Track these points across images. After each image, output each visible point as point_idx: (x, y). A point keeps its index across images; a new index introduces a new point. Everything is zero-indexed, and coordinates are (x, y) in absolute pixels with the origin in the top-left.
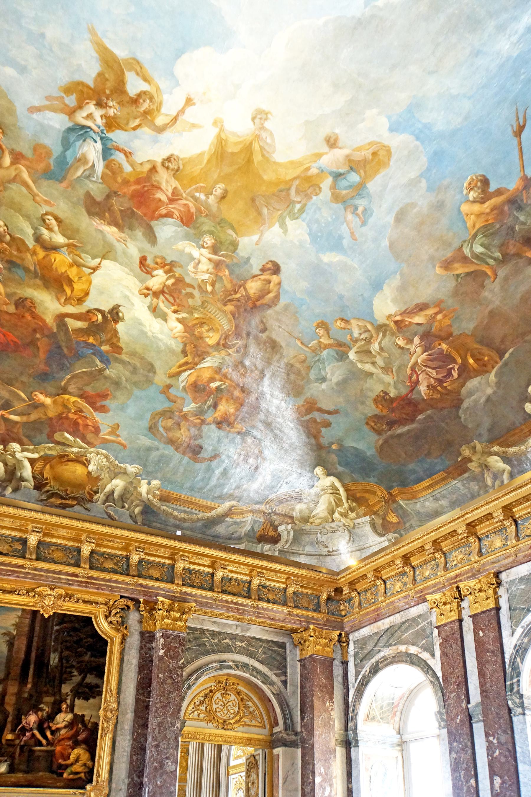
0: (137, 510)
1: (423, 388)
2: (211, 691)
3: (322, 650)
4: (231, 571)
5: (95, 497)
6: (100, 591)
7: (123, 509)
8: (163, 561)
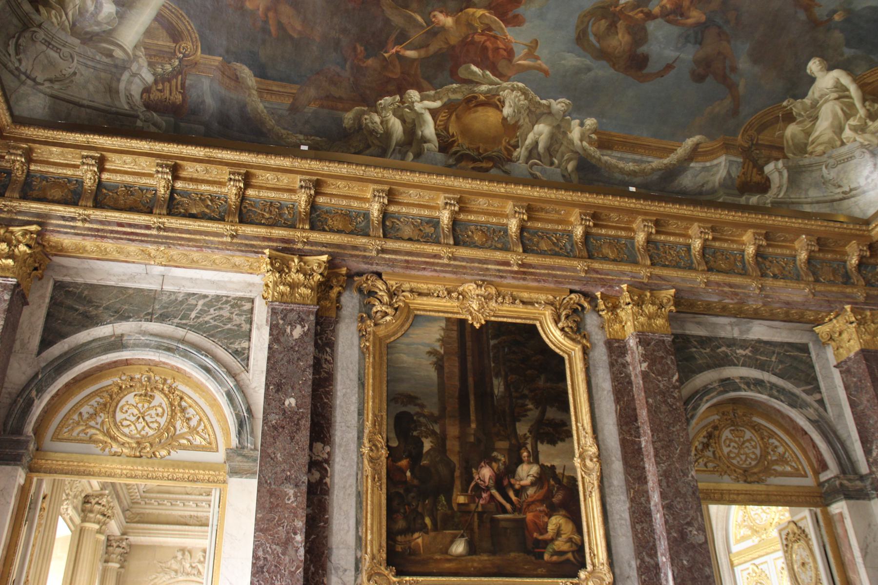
0: (570, 167)
2: (715, 428)
5: (515, 154)
6: (542, 284)
7: (553, 168)
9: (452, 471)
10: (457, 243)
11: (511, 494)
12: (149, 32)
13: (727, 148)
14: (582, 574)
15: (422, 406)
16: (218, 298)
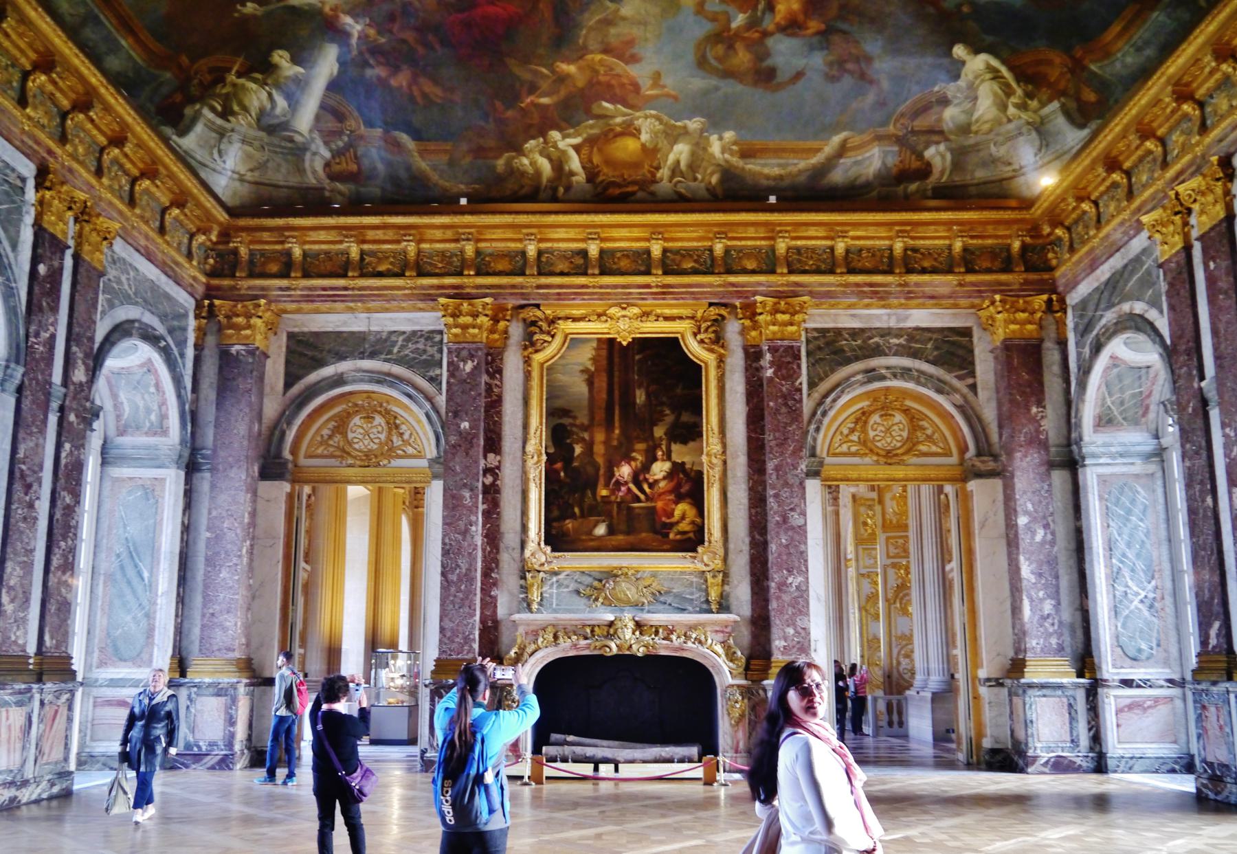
3: (1021, 330)
4: (853, 238)
8: (758, 243)
9: (598, 470)
11: (646, 487)
12: (318, 118)
13: (879, 138)
14: (700, 549)
15: (575, 418)
16: (414, 333)
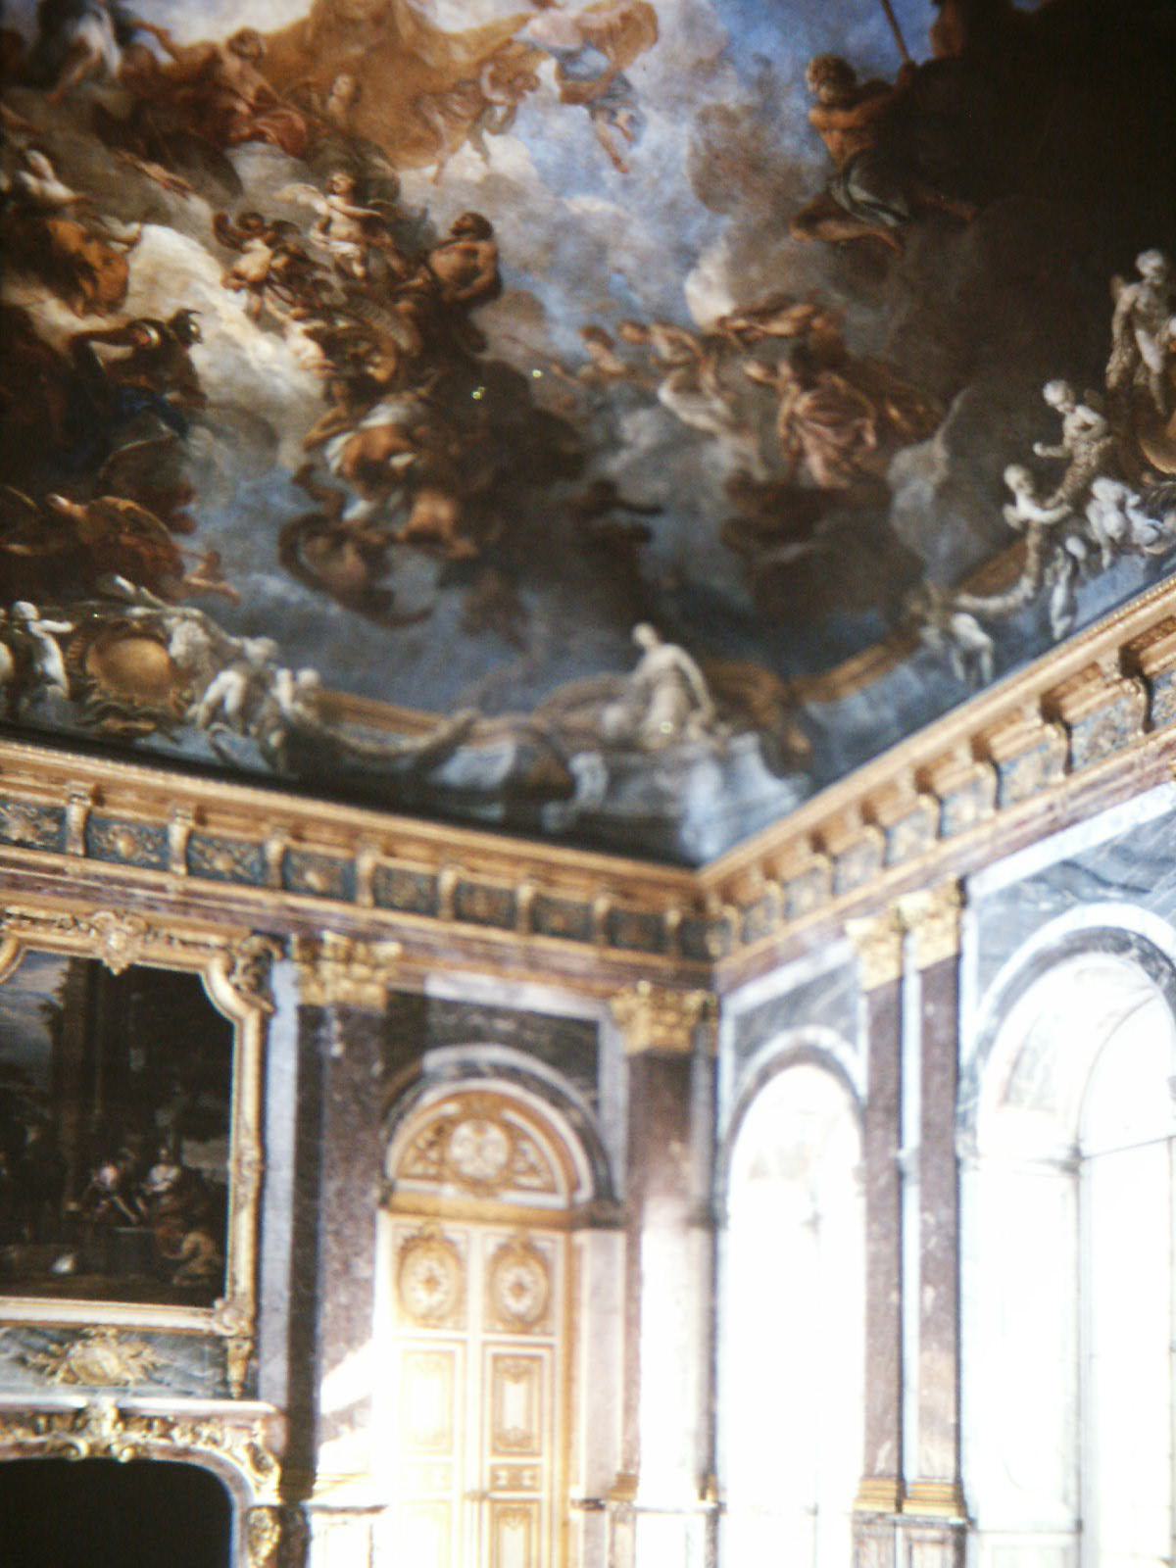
1: (816, 466)
10: (89, 854)
11: (140, 1204)
